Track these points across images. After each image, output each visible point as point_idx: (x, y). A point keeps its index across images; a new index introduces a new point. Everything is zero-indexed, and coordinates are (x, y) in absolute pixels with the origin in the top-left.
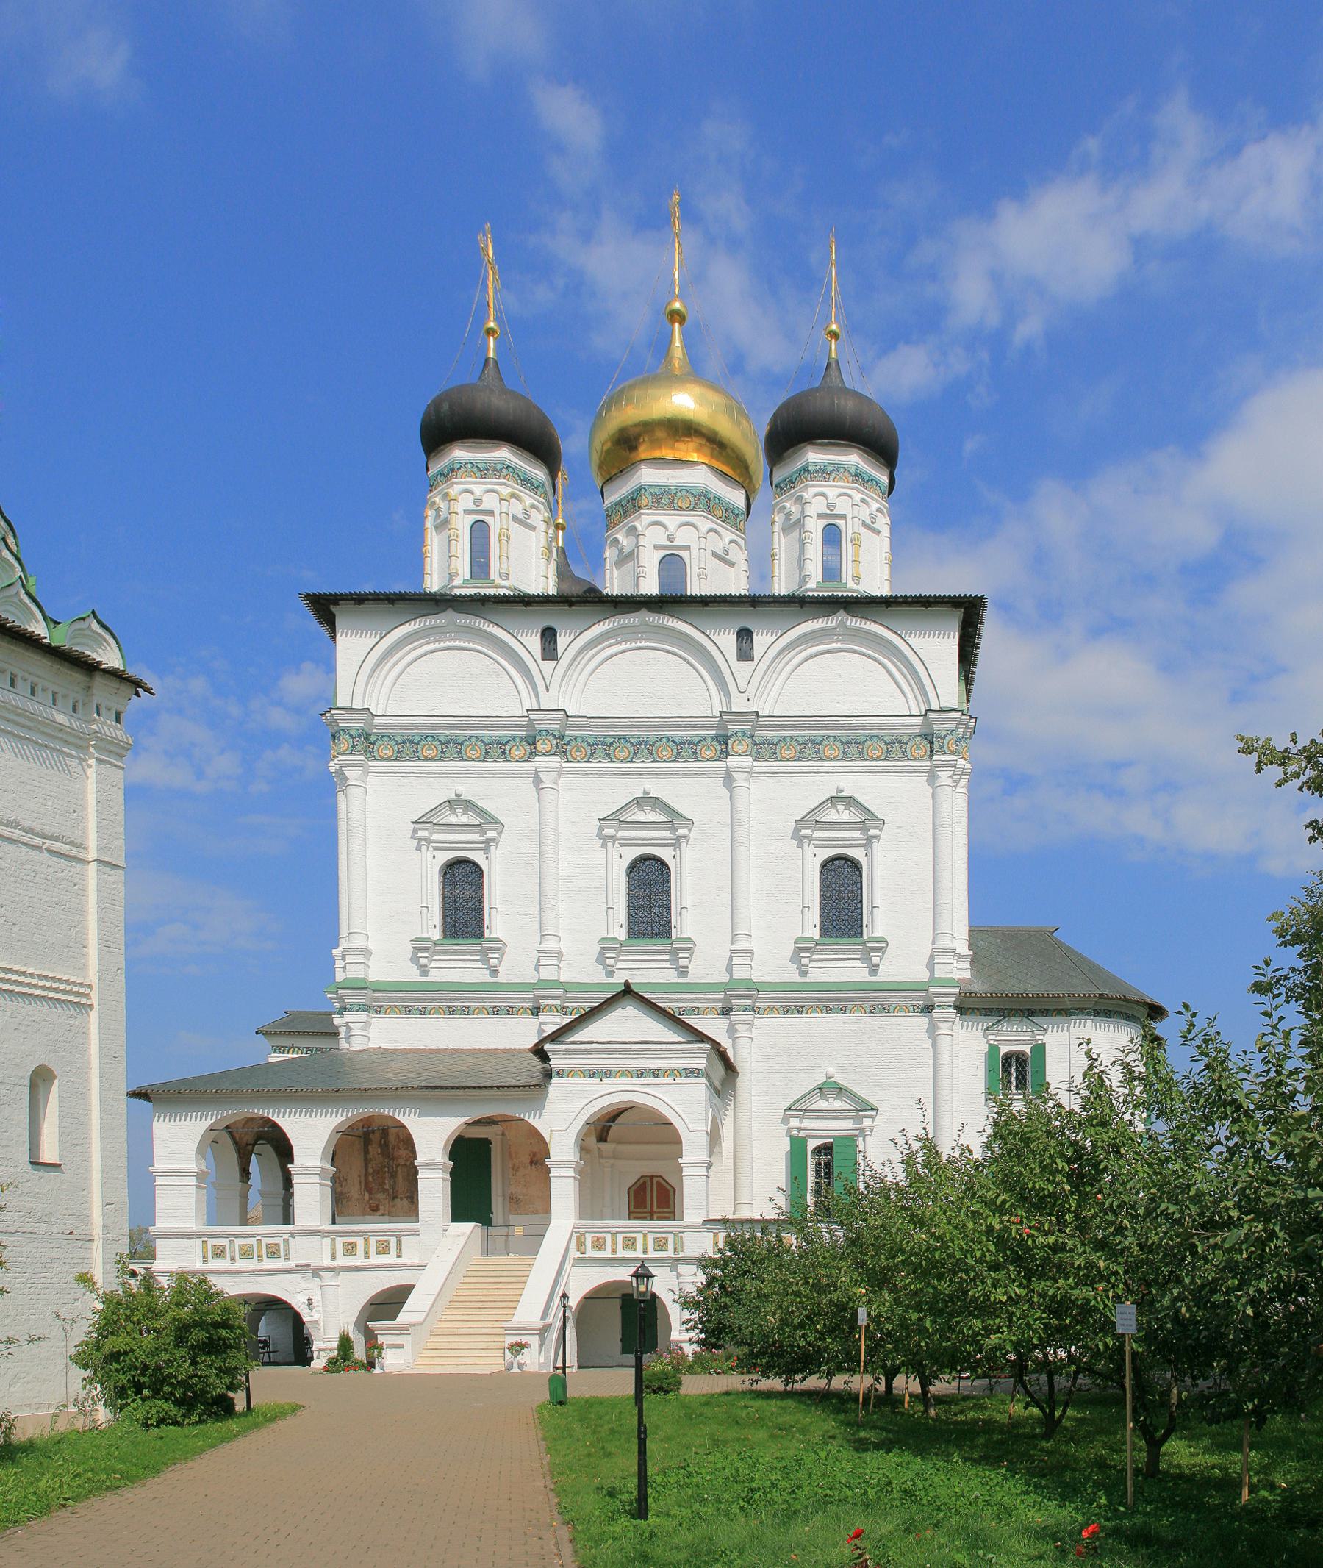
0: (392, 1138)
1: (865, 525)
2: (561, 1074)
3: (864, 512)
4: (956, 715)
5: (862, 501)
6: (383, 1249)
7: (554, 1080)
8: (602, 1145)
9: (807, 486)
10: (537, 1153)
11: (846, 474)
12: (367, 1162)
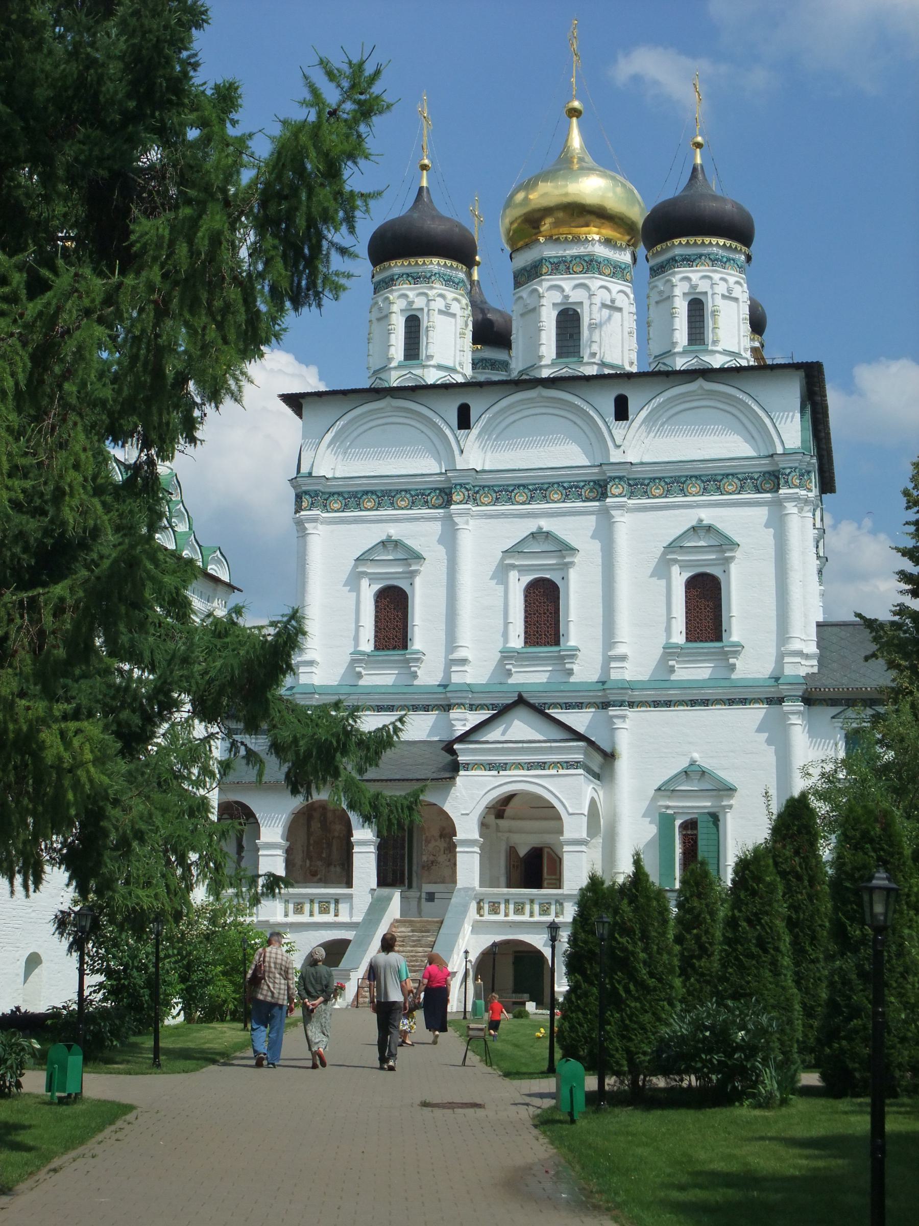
0: (329, 815)
1: (723, 296)
2: (467, 767)
3: (721, 288)
4: (799, 457)
5: (722, 279)
6: (324, 910)
7: (461, 773)
8: (501, 822)
9: (675, 273)
10: (448, 830)
11: (708, 261)
12: (309, 834)
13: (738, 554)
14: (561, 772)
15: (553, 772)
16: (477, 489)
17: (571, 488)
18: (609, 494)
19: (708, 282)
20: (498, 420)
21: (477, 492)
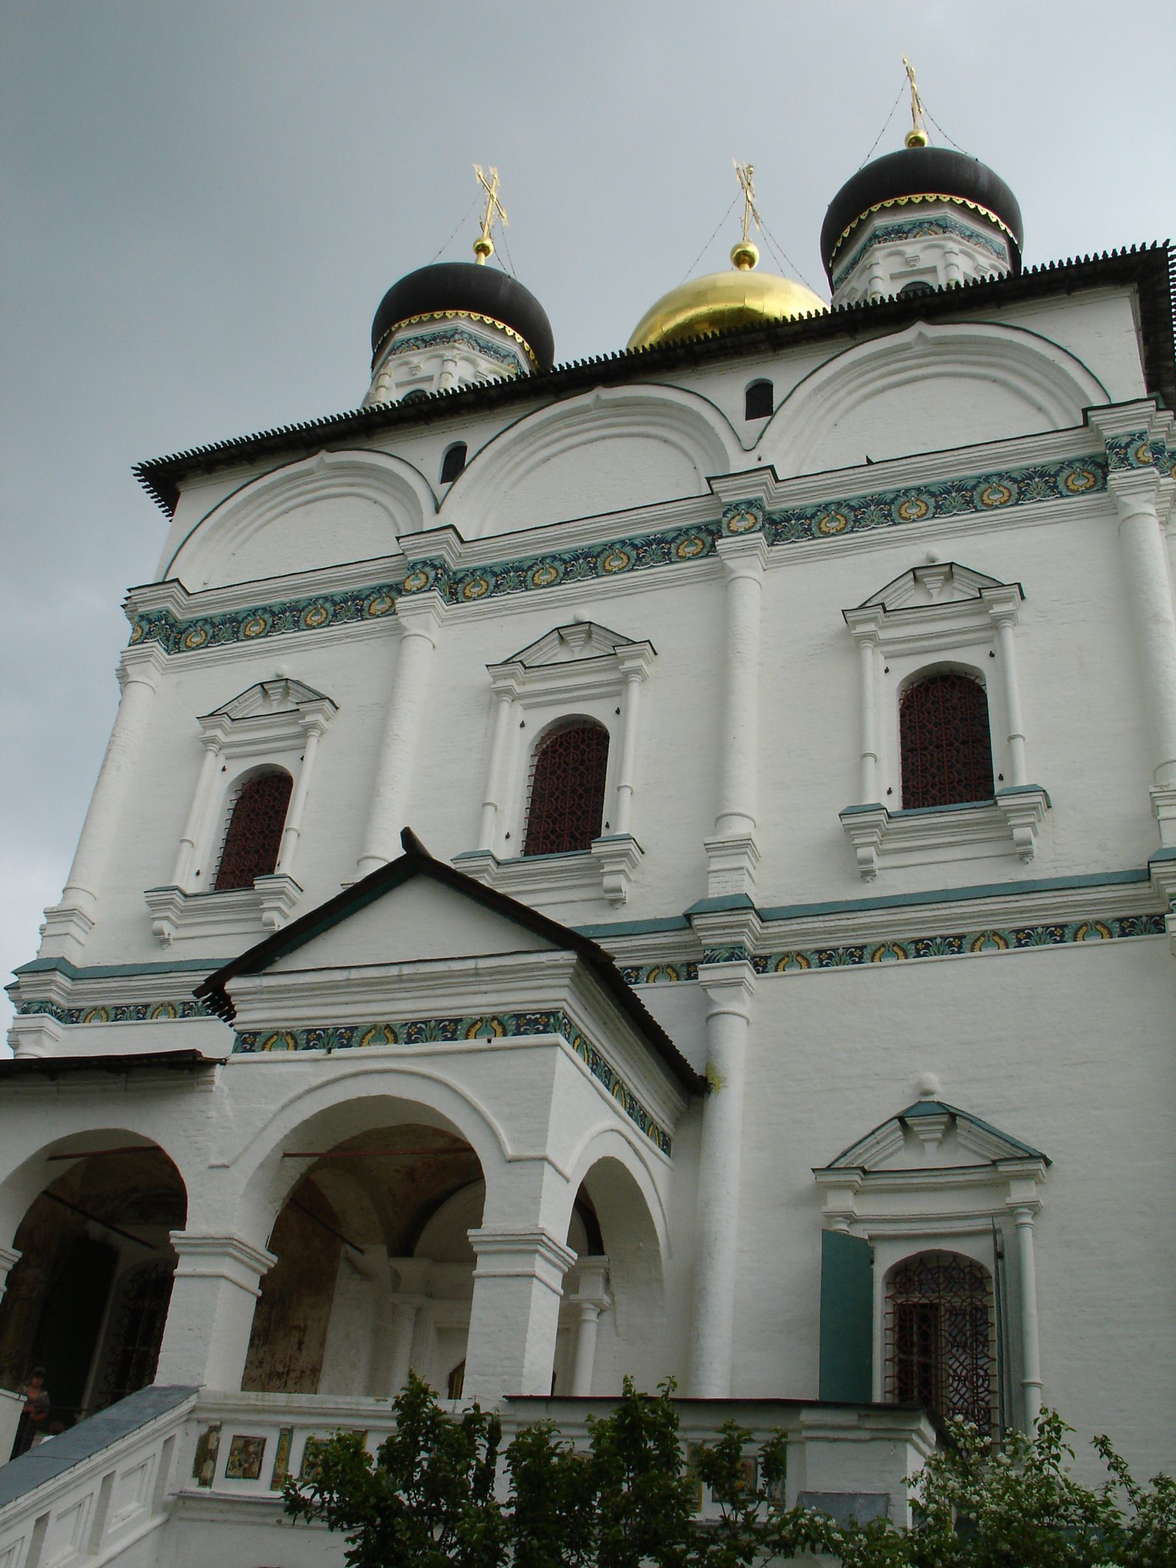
13: (1025, 613)
14: (499, 1041)
15: (481, 1043)
16: (460, 575)
17: (649, 544)
18: (725, 532)
19: (938, 251)
20: (517, 459)
21: (461, 580)
